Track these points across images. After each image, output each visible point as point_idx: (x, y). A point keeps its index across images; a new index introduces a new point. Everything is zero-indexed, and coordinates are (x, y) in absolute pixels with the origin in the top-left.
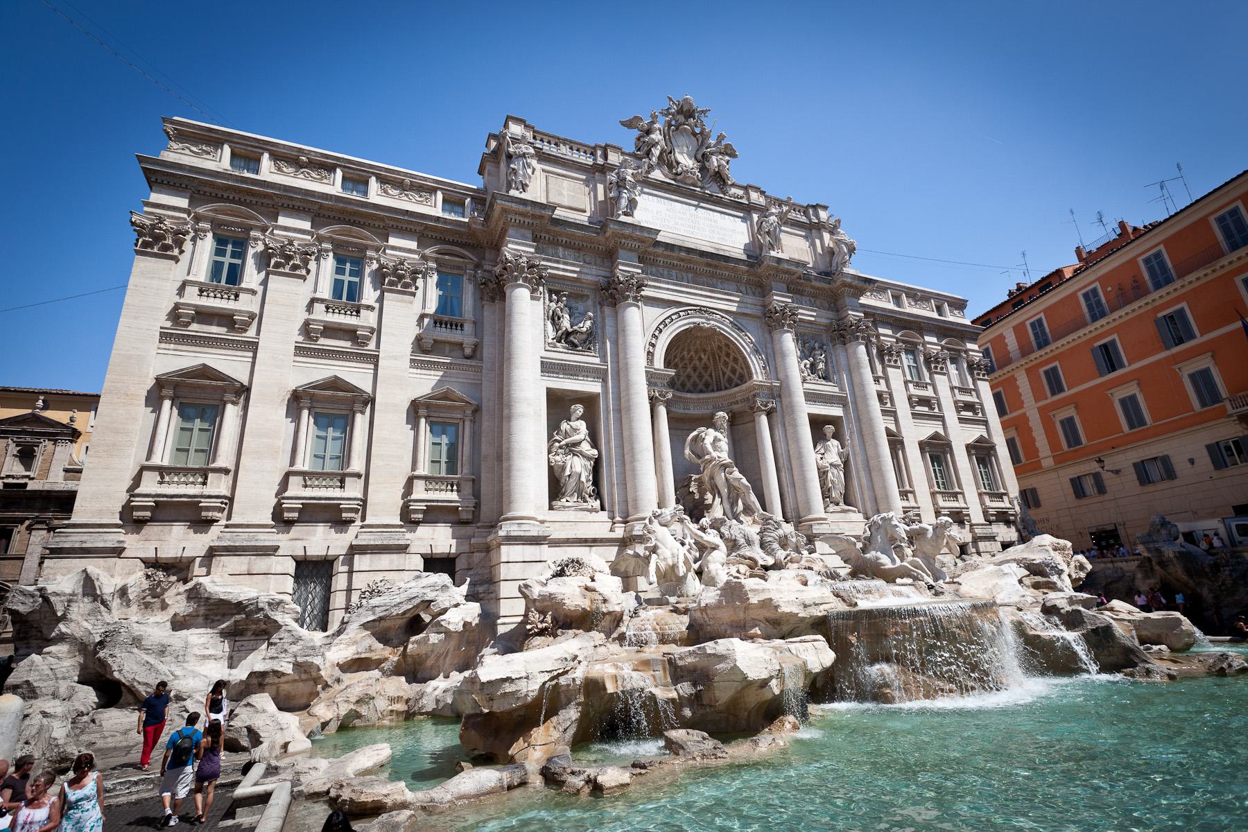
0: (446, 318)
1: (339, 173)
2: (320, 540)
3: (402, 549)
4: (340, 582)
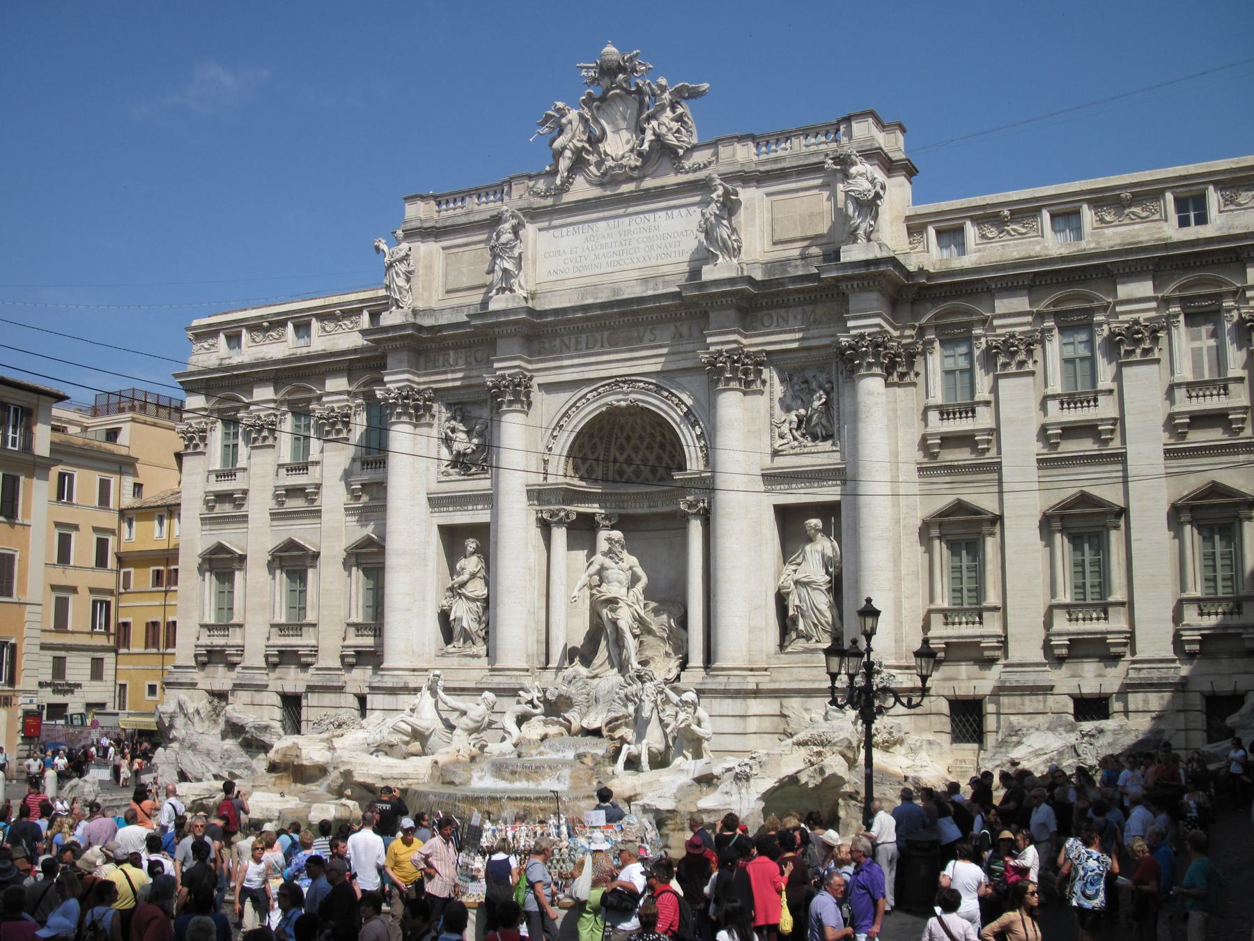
0: (370, 458)
1: (290, 325)
2: (293, 680)
3: (340, 689)
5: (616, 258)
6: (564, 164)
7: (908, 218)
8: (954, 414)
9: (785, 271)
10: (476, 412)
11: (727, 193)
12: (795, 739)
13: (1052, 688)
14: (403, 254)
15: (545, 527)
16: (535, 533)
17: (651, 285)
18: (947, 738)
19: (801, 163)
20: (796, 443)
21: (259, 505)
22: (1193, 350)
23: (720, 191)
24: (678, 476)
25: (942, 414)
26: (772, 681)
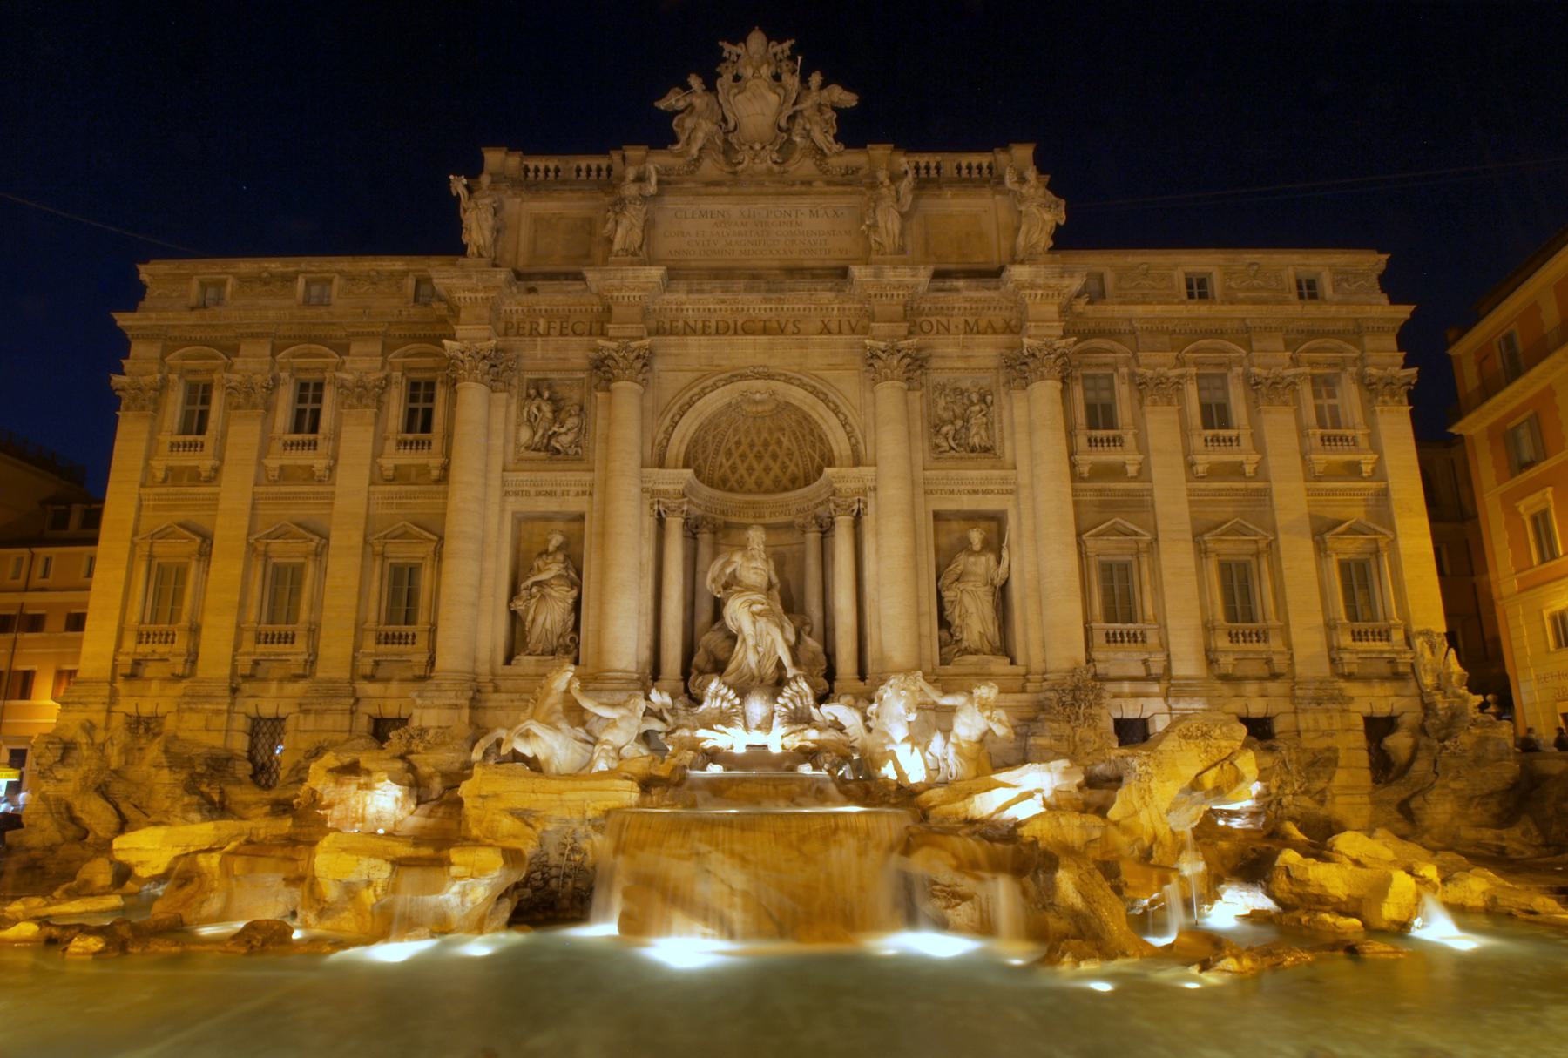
1: (301, 281)
15: (661, 522)
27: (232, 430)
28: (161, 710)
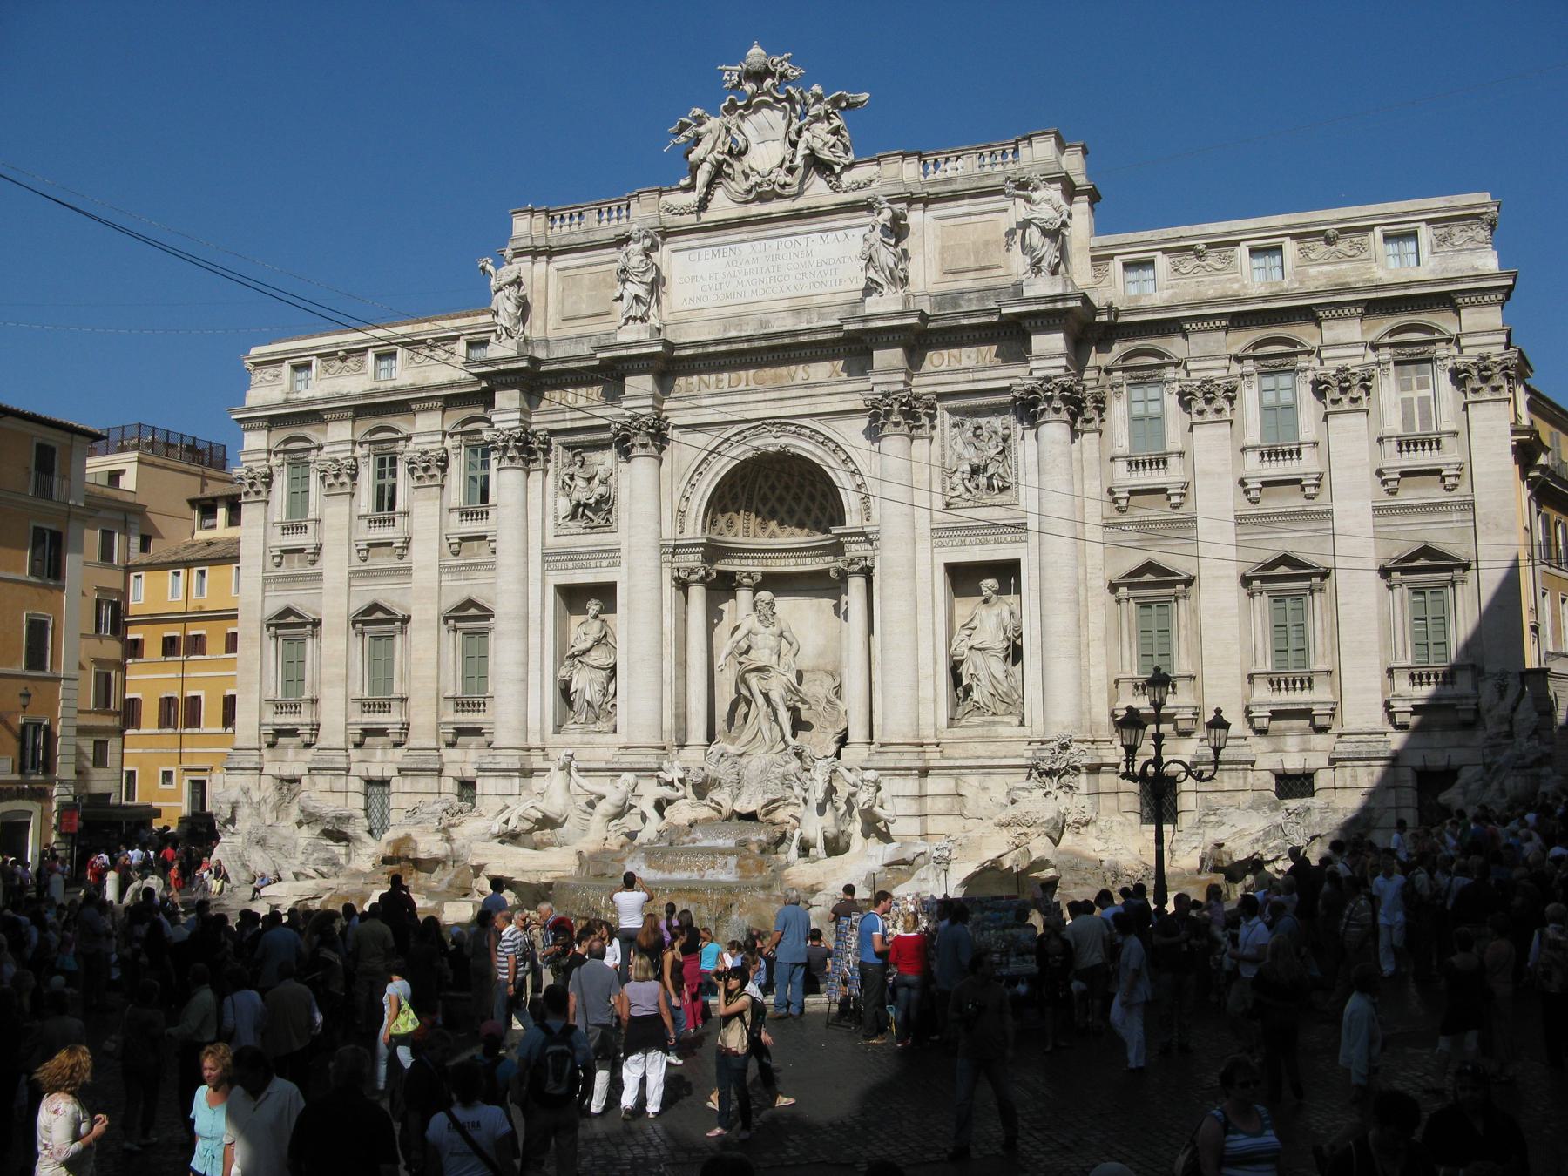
2: (382, 761)
4: (394, 801)
5: (763, 286)
6: (702, 176)
7: (1092, 249)
8: (1144, 464)
9: (956, 305)
10: (595, 457)
11: (897, 219)
12: (996, 820)
13: (1253, 763)
14: (513, 276)
15: (682, 585)
16: (669, 591)
17: (804, 317)
18: (1135, 818)
19: (974, 185)
20: (968, 496)
21: (335, 563)
22: (1403, 401)
23: (887, 214)
24: (836, 530)
25: (1130, 464)
26: (943, 758)
27: (328, 511)
28: (298, 773)
